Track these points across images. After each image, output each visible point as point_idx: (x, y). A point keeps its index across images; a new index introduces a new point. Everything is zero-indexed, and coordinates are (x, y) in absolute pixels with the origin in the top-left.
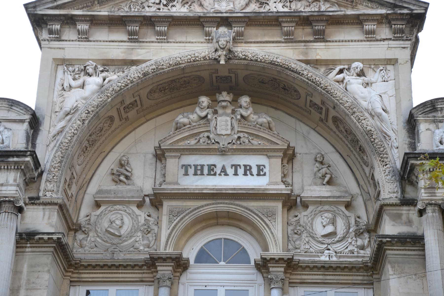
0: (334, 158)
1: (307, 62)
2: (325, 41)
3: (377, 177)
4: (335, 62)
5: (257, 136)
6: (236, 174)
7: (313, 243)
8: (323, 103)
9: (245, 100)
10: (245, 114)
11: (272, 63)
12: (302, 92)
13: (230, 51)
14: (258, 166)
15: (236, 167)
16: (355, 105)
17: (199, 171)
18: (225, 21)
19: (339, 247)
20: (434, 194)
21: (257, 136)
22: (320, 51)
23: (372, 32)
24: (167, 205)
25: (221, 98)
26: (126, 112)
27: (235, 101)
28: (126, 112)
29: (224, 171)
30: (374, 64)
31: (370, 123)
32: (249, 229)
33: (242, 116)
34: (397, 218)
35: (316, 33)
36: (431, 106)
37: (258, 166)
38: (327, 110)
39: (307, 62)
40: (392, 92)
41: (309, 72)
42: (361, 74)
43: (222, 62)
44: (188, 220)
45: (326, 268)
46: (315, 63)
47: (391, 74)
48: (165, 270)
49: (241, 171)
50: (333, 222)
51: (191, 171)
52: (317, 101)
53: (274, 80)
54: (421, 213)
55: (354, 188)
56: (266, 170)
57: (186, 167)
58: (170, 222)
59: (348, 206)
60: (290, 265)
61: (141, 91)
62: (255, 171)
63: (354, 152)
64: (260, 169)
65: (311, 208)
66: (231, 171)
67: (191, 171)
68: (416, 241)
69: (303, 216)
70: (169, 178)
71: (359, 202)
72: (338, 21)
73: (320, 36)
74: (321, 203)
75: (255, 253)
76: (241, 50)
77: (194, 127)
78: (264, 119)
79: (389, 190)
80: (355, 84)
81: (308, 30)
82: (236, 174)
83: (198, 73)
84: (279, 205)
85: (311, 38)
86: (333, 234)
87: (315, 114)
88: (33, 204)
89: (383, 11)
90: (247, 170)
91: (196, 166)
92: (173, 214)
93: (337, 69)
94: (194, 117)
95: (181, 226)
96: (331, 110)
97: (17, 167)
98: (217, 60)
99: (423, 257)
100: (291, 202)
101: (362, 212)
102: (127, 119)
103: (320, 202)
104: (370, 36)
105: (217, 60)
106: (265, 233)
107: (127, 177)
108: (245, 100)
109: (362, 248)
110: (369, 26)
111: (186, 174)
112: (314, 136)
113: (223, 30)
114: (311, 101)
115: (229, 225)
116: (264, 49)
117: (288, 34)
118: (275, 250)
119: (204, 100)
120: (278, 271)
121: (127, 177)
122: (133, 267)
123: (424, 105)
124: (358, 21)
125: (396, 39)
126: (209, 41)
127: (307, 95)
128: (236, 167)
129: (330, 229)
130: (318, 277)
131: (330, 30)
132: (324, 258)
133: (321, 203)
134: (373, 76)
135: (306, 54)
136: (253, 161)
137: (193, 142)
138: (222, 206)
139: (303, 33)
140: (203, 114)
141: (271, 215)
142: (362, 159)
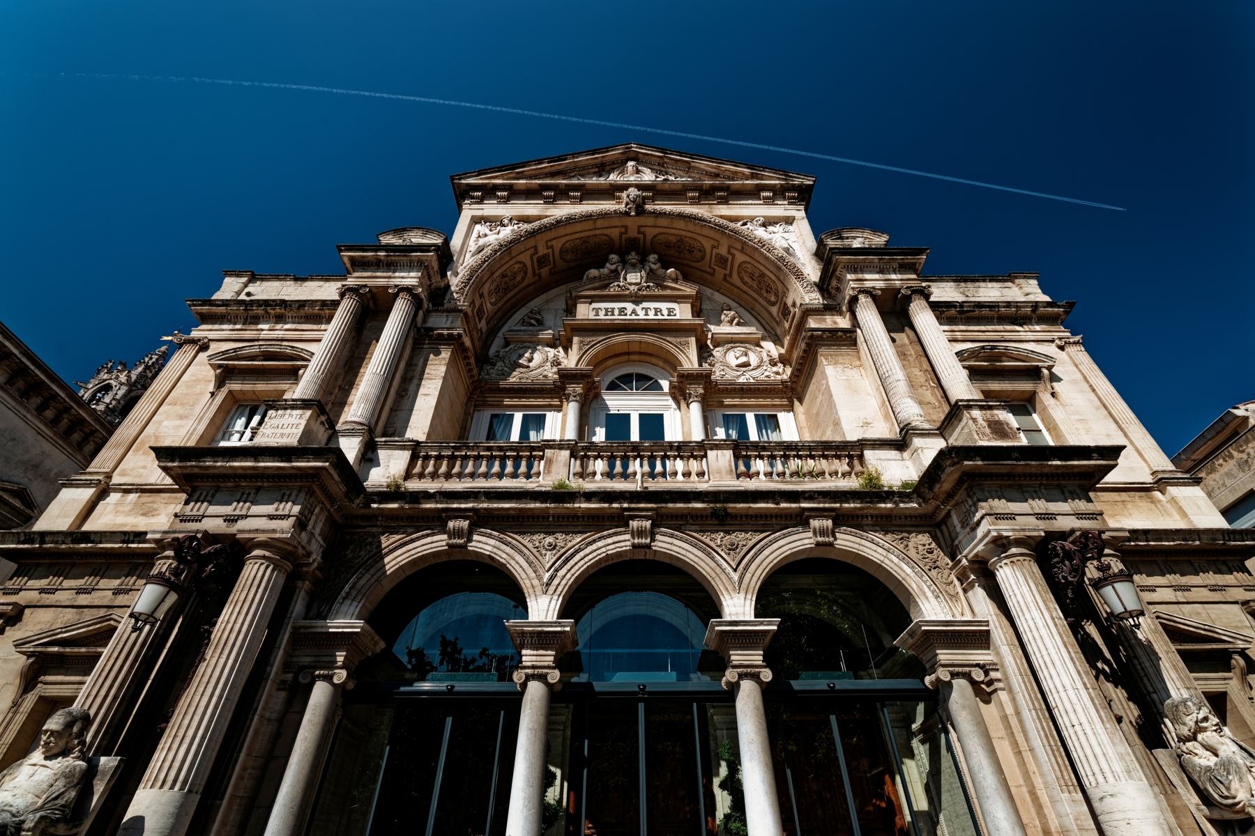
7: (728, 370)
10: (654, 267)
14: (669, 309)
22: (724, 210)
26: (540, 267)
28: (540, 267)
32: (661, 364)
33: (651, 270)
37: (669, 309)
53: (681, 240)
58: (580, 349)
61: (554, 242)
63: (761, 300)
73: (724, 201)
74: (732, 341)
83: (607, 232)
86: (746, 365)
87: (720, 272)
88: (437, 311)
91: (606, 310)
94: (605, 271)
96: (738, 254)
97: (420, 265)
98: (627, 214)
102: (540, 275)
104: (769, 201)
106: (680, 357)
107: (537, 320)
108: (653, 257)
114: (717, 254)
119: (614, 257)
121: (537, 320)
127: (713, 247)
129: (743, 359)
132: (741, 380)
133: (732, 341)
140: (613, 267)
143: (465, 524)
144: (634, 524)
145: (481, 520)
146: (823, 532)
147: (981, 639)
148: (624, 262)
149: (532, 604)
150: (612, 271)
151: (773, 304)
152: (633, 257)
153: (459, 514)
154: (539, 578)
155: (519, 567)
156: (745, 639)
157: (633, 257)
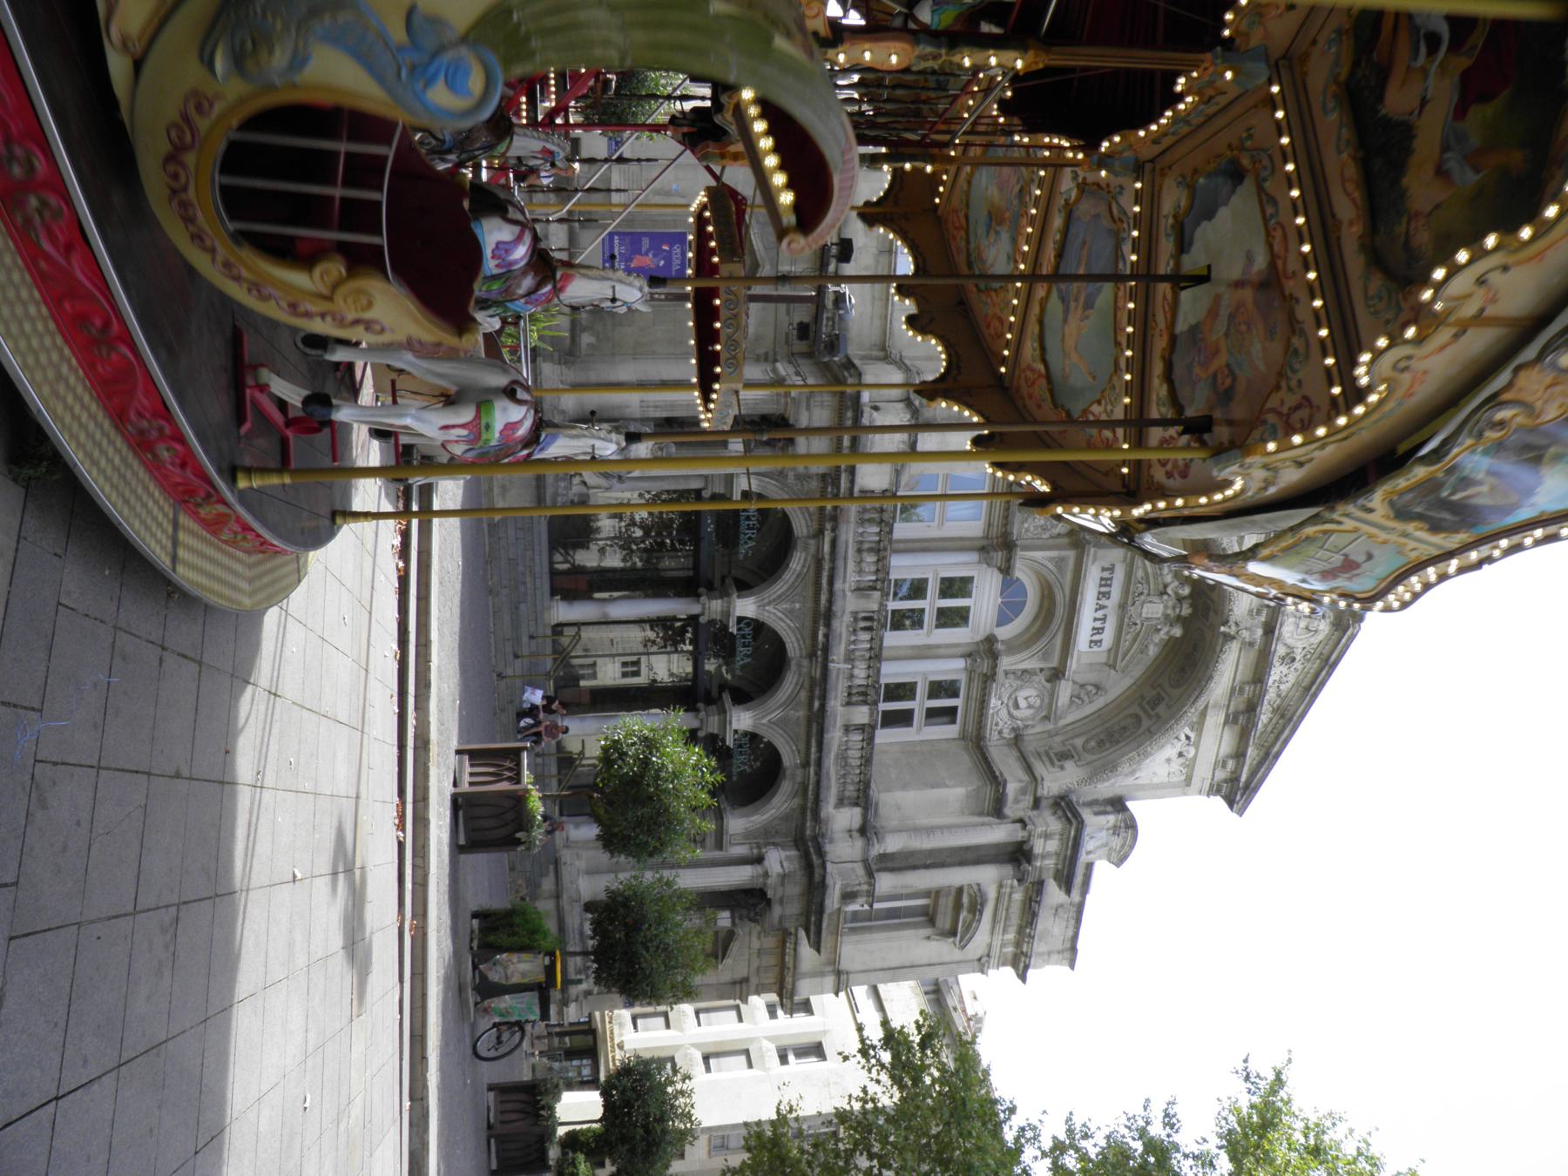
0: (1100, 702)
1: (1206, 707)
2: (1226, 722)
3: (1069, 764)
4: (1199, 735)
5: (1135, 640)
6: (1095, 619)
7: (1010, 690)
8: (1158, 716)
9: (1177, 632)
11: (1211, 678)
12: (1175, 692)
13: (1233, 638)
15: (1104, 619)
16: (1147, 755)
17: (1105, 582)
18: (1270, 629)
19: (1004, 713)
20: (1040, 836)
21: (1135, 640)
22: (1215, 720)
23: (1224, 765)
24: (1071, 555)
25: (1185, 606)
27: (1179, 618)
29: (1102, 607)
30: (1190, 766)
31: (1125, 768)
32: (1033, 630)
34: (1023, 791)
35: (1236, 715)
36: (1131, 825)
38: (1149, 716)
39: (1206, 707)
40: (1156, 780)
41: (1192, 714)
42: (1180, 755)
43: (1222, 629)
44: (1051, 578)
45: (983, 703)
46: (1203, 714)
47: (1175, 779)
48: (999, 557)
49: (1098, 624)
50: (1030, 706)
51: (1106, 575)
52: (1161, 709)
54: (1021, 821)
55: (1062, 723)
56: (1095, 649)
57: (1111, 569)
58: (1050, 559)
59: (1047, 718)
60: (989, 678)
62: (1096, 638)
64: (1098, 643)
65: (1048, 685)
66: (1100, 614)
67: (1106, 575)
68: (997, 810)
69: (1041, 678)
70: (1101, 552)
71: (1050, 726)
72: (1244, 737)
73: (1231, 720)
75: (1004, 633)
76: (1234, 647)
77: (1155, 578)
78: (1153, 651)
79: (1054, 781)
80: (1170, 751)
81: (1242, 707)
82: (1095, 619)
84: (1054, 663)
85: (1232, 709)
86: (1017, 706)
89: (1243, 778)
90: (1098, 631)
92: (1059, 562)
93: (1192, 735)
94: (1168, 578)
95: (1045, 572)
98: (1225, 623)
99: (981, 814)
100: (1057, 675)
101: (1039, 729)
103: (1053, 695)
105: (1225, 623)
108: (1177, 632)
109: (1000, 732)
110: (1231, 764)
111: (1104, 569)
112: (1127, 682)
113: (1260, 632)
115: (1041, 607)
116: (1229, 668)
117: (1241, 690)
118: (1006, 663)
120: (985, 667)
122: (1006, 517)
123: (1133, 819)
124: (1239, 755)
125: (1211, 786)
126: (1251, 611)
128: (1104, 619)
129: (1023, 704)
130: (975, 693)
131: (1237, 728)
132: (994, 702)
134: (1176, 765)
135: (1215, 706)
136: (1108, 638)
137: (1140, 574)
138: (1060, 611)
139: (1239, 703)
140: (1169, 591)
141: (1046, 656)
142: (1092, 738)
143: (812, 550)
144: (805, 662)
145: (819, 562)
146: (793, 775)
147: (719, 845)
148: (1180, 599)
149: (751, 600)
150: (1165, 586)
151: (1086, 742)
152: (1186, 610)
153: (819, 549)
154: (769, 603)
155: (779, 587)
156: (724, 724)
157: (1186, 610)
